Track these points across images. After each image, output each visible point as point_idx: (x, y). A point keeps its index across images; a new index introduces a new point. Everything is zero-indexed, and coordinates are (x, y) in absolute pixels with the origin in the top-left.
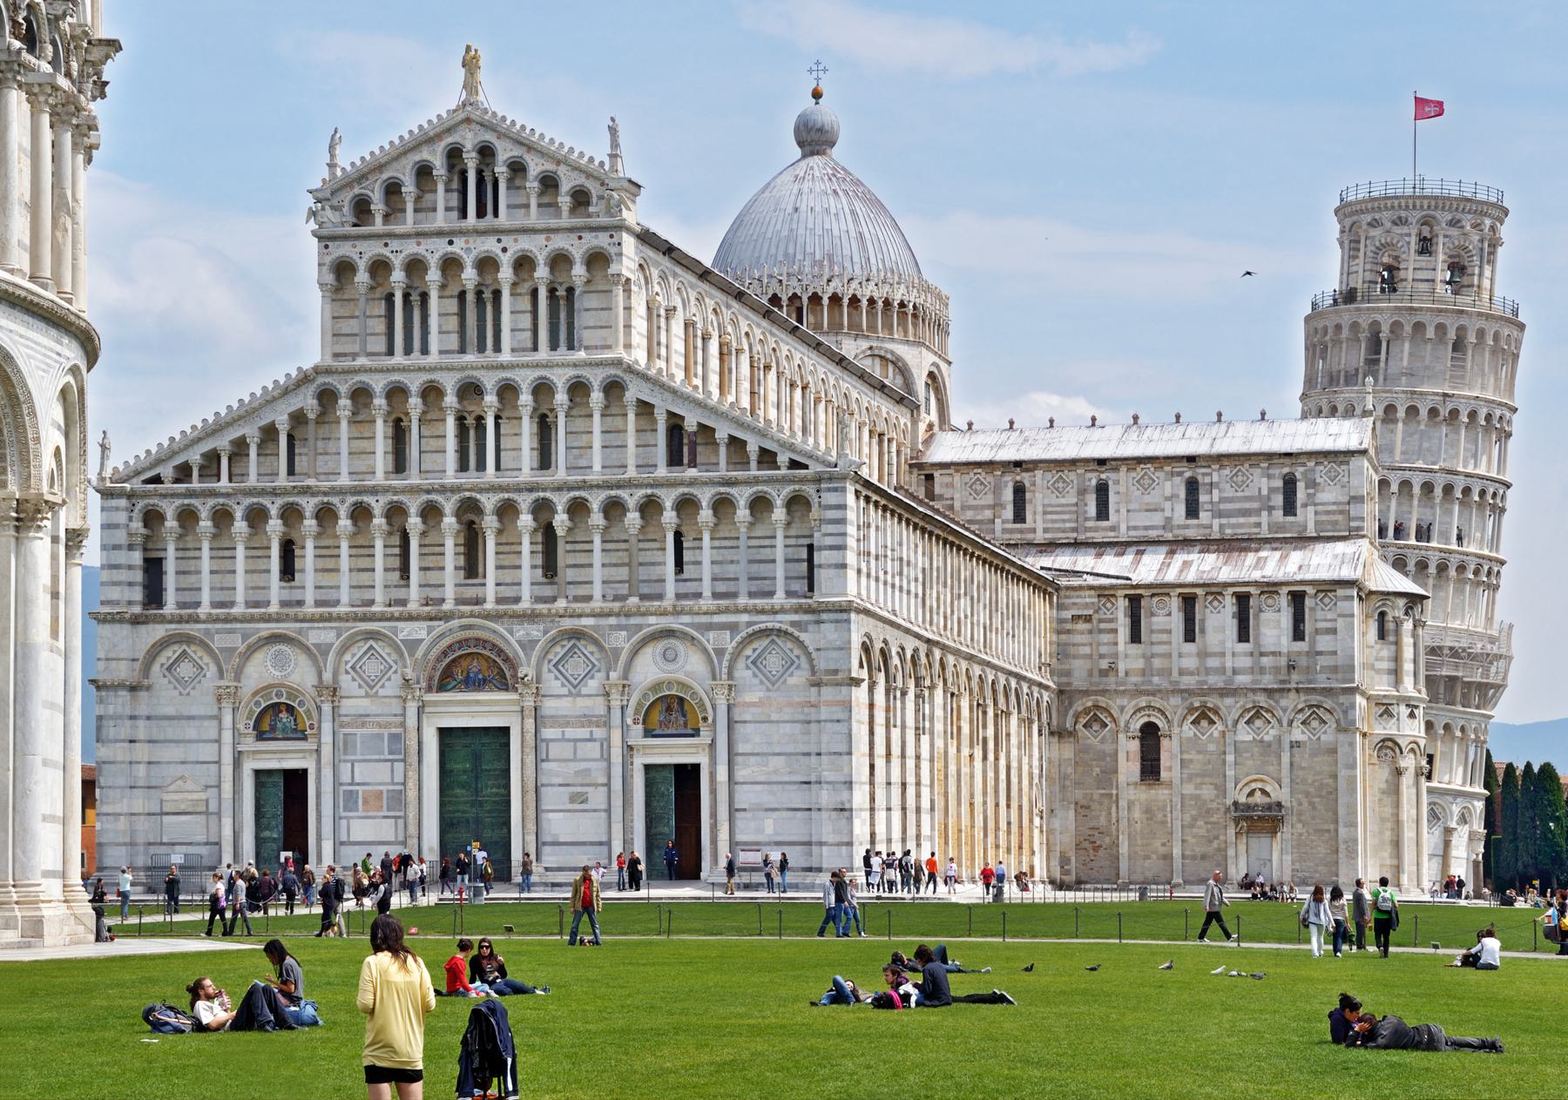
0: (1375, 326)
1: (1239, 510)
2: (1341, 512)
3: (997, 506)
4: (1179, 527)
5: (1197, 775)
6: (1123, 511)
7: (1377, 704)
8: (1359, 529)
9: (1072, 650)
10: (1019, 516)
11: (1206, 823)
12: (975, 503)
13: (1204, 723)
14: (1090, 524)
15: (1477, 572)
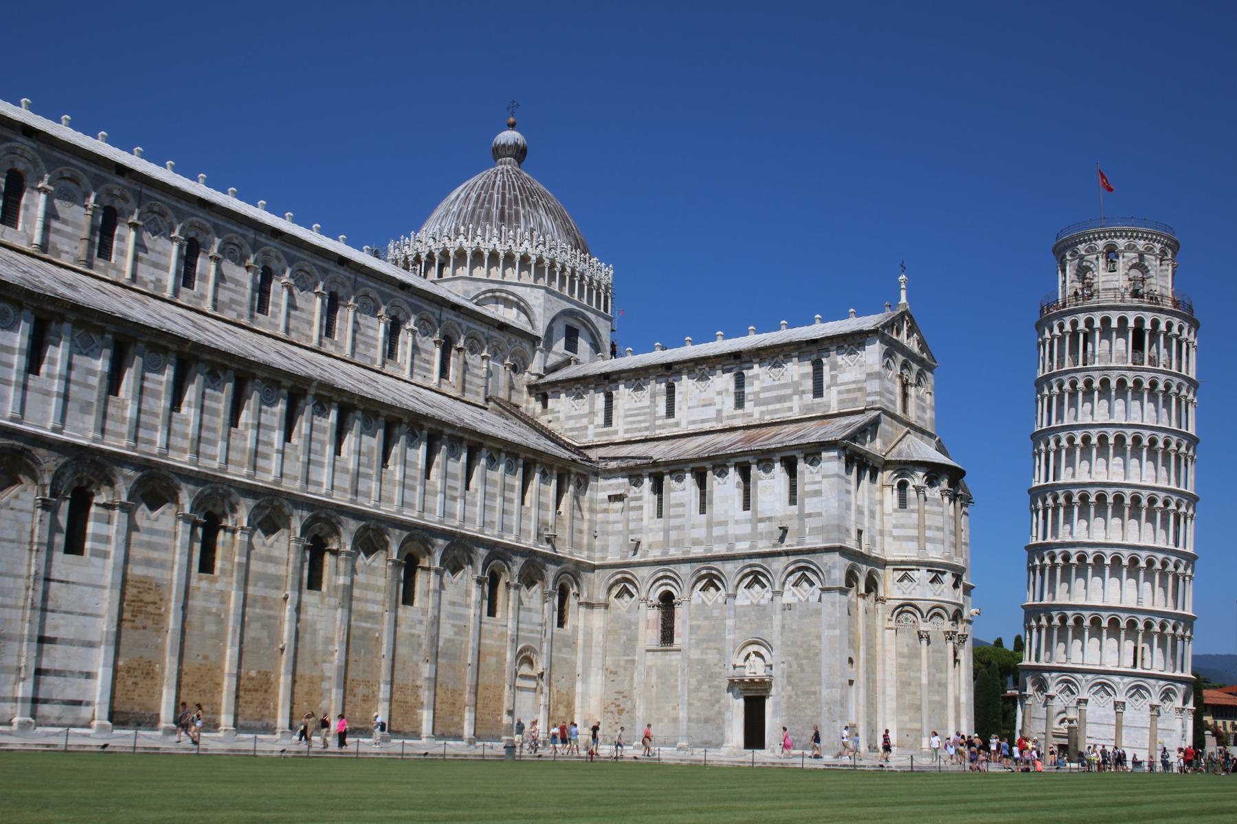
0: (1074, 324)
1: (776, 397)
2: (860, 389)
3: (592, 413)
4: (728, 418)
5: (704, 640)
6: (685, 408)
7: (894, 570)
8: (873, 402)
9: (610, 528)
10: (608, 421)
11: (710, 687)
12: (576, 413)
13: (712, 590)
14: (658, 422)
15: (1166, 503)
